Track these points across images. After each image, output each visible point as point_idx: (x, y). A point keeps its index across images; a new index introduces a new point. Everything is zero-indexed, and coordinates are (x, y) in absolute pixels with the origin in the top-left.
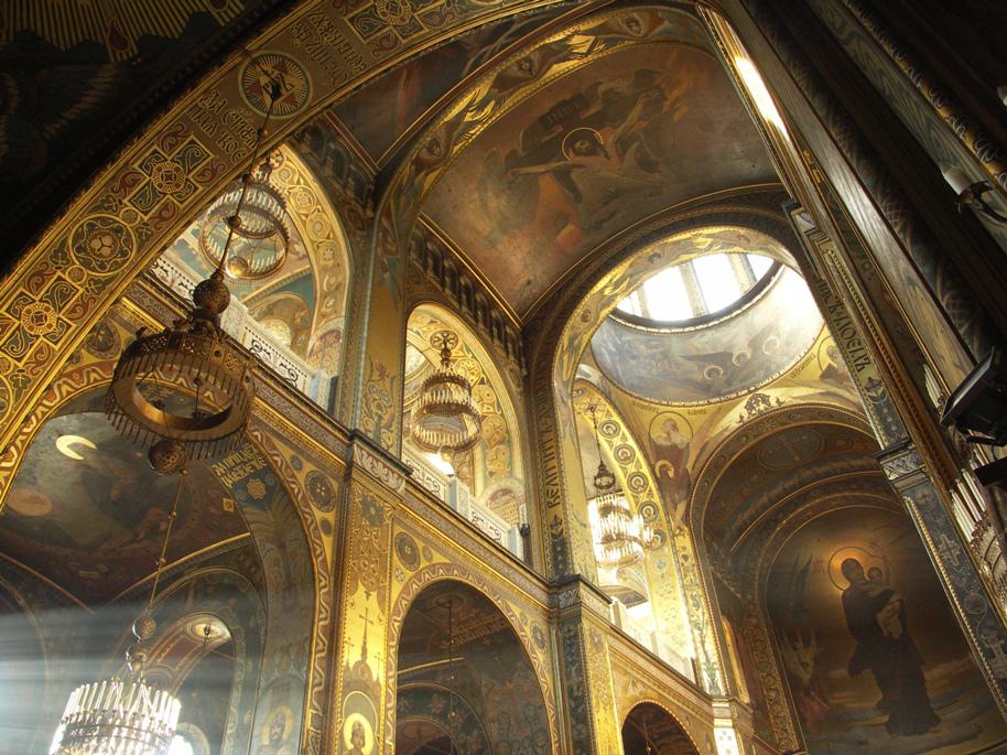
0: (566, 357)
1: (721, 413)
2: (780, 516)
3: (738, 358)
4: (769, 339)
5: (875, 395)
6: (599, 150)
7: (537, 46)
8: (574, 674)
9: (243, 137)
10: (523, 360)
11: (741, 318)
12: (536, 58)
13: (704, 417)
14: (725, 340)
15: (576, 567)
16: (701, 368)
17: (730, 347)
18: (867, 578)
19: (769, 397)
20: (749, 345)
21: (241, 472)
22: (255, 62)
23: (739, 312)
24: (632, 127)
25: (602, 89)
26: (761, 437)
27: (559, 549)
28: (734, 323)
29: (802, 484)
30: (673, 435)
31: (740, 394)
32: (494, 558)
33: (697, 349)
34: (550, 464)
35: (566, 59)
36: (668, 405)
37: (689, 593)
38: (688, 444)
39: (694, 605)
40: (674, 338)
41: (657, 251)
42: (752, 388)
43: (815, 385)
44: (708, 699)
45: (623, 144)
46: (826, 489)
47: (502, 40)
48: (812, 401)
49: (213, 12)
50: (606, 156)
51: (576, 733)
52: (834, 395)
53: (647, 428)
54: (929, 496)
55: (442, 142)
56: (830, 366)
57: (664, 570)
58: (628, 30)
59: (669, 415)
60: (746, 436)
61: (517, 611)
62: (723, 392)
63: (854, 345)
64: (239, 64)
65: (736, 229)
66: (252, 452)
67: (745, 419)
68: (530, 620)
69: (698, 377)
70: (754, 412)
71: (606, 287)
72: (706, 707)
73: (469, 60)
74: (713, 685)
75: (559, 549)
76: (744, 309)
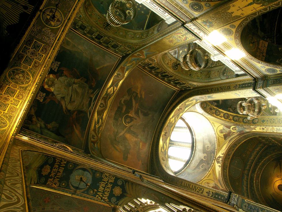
1: (214, 171)
3: (204, 158)
6: (132, 118)
7: (101, 99)
9: (50, 36)
11: (196, 152)
12: (103, 102)
13: (212, 175)
14: (198, 159)
16: (199, 168)
20: (204, 153)
21: (108, 190)
22: (44, 13)
23: (194, 151)
24: (135, 107)
25: (122, 102)
26: (228, 167)
29: (248, 175)
30: (209, 185)
33: (193, 167)
34: (191, 187)
36: (201, 180)
40: (187, 170)
41: (165, 132)
43: (226, 142)
45: (137, 113)
46: (253, 172)
47: (92, 104)
48: (230, 145)
49: (26, 11)
50: (135, 119)
52: (231, 139)
55: (95, 135)
56: (224, 135)
58: (118, 78)
59: (204, 182)
60: (225, 169)
62: (209, 166)
64: (39, 16)
65: (176, 108)
66: (107, 177)
67: (220, 165)
69: (201, 170)
70: (220, 162)
71: (161, 149)
73: (87, 113)
75: (217, 196)
76: (194, 149)
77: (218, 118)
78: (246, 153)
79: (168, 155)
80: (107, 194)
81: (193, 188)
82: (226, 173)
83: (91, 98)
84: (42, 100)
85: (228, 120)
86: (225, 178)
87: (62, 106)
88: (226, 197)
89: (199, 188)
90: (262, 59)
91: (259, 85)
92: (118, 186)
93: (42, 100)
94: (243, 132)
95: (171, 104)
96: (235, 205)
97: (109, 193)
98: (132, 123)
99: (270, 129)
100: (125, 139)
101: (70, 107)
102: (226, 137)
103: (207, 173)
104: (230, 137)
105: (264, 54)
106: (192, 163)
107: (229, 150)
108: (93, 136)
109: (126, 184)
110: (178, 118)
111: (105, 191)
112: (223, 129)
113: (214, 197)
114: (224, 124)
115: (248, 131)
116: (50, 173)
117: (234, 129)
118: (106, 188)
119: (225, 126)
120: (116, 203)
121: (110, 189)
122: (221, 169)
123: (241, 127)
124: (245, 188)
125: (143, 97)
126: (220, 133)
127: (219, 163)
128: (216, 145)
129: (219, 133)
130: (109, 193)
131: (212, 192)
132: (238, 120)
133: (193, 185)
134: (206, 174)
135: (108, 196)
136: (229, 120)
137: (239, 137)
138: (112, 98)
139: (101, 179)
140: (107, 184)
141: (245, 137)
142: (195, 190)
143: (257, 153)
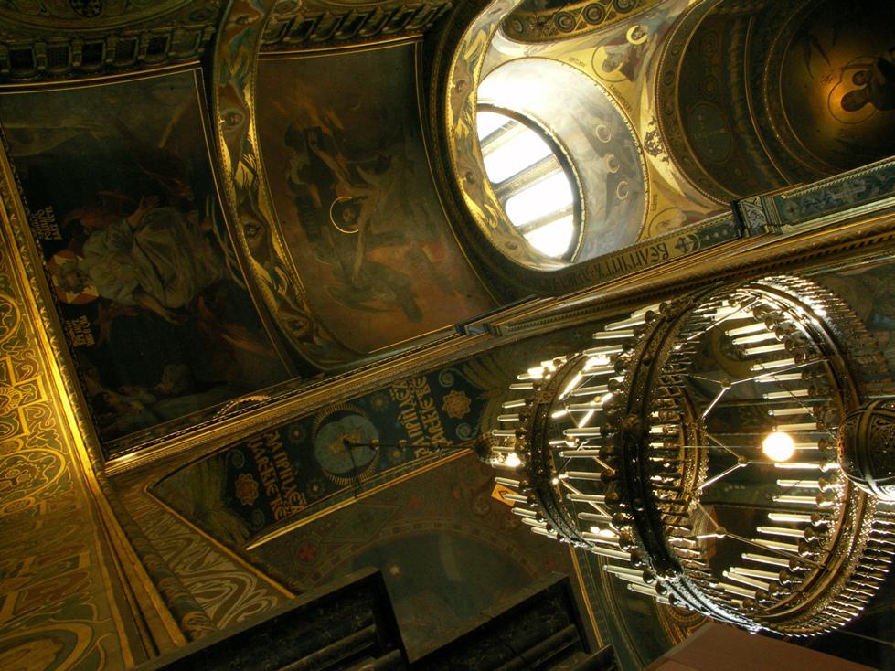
1: (658, 181)
2: (784, 155)
3: (612, 166)
4: (598, 135)
7: (236, 215)
8: (839, 196)
11: (580, 167)
12: (247, 220)
13: (661, 197)
14: (596, 181)
16: (618, 203)
17: (603, 175)
19: (647, 133)
21: (431, 419)
25: (296, 181)
28: (584, 174)
29: (751, 132)
31: (643, 162)
33: (600, 209)
34: (629, 262)
35: (256, 195)
36: (643, 229)
38: (685, 212)
40: (589, 230)
41: (464, 173)
43: (640, 85)
45: (355, 180)
46: (759, 111)
47: (224, 246)
48: (654, 86)
55: (295, 317)
56: (622, 70)
58: (237, 126)
60: (683, 158)
62: (639, 178)
65: (449, 90)
66: (403, 390)
69: (624, 204)
70: (660, 148)
71: (488, 225)
73: (232, 280)
75: (708, 238)
76: (571, 164)
77: (576, 36)
78: (712, 75)
79: (514, 227)
80: (437, 430)
81: (636, 261)
82: (693, 163)
83: (210, 234)
84: (91, 340)
85: (607, 23)
86: (700, 181)
87: (153, 314)
88: (732, 224)
92: (447, 391)
93: (91, 340)
94: (668, 26)
95: (426, 91)
97: (439, 424)
98: (364, 214)
100: (376, 269)
101: (175, 300)
102: (629, 71)
103: (646, 199)
104: (642, 63)
106: (591, 203)
107: (661, 101)
108: (293, 324)
109: (463, 372)
110: (470, 113)
111: (426, 427)
112: (611, 55)
115: (677, 13)
116: (262, 489)
117: (637, 34)
118: (424, 418)
120: (474, 434)
121: (435, 413)
122: (674, 163)
123: (654, 14)
124: (763, 168)
125: (339, 125)
127: (658, 154)
128: (620, 112)
130: (439, 424)
131: (691, 237)
132: (632, 3)
133: (631, 255)
134: (646, 204)
135: (442, 433)
136: (608, 19)
137: (665, 46)
138: (262, 189)
139: (395, 409)
140: (418, 408)
141: (681, 35)
142: (643, 262)
143: (740, 56)
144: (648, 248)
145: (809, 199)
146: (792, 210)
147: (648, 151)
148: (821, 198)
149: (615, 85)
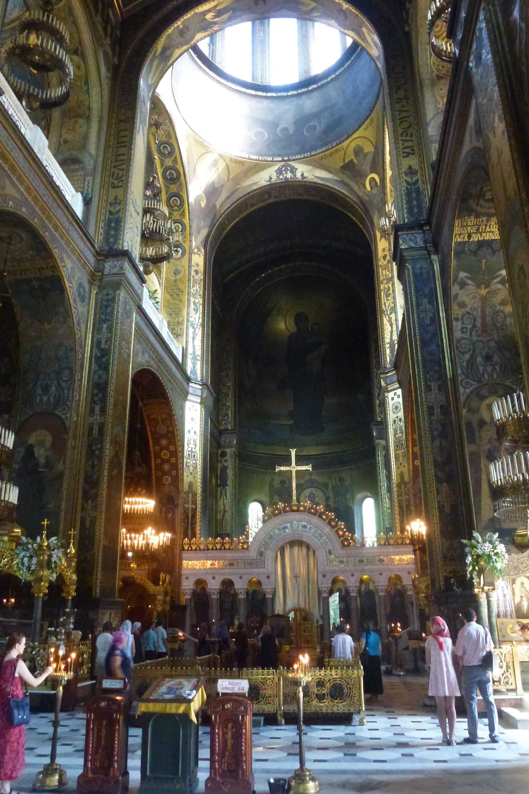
0: (155, 63)
5: (409, 180)
8: (104, 330)
10: (117, 48)
11: (294, 99)
15: (125, 244)
18: (310, 329)
19: (297, 169)
27: (113, 225)
31: (275, 159)
32: (60, 210)
37: (192, 299)
39: (194, 309)
42: (286, 158)
44: (188, 380)
51: (96, 377)
53: (195, 160)
54: (425, 268)
56: (351, 162)
57: (178, 277)
61: (69, 265)
63: (406, 135)
67: (273, 180)
68: (78, 275)
70: (281, 177)
71: (209, 11)
72: (185, 384)
74: (194, 371)
76: (300, 91)
88: (115, 247)
89: (122, 172)
90: (460, 235)
91: (413, 238)
96: (100, 274)
99: (387, 273)
105: (475, 238)
112: (366, 155)
113: (109, 218)
114: (378, 153)
117: (374, 183)
119: (374, 156)
122: (264, 186)
126: (354, 150)
127: (277, 174)
129: (353, 145)
131: (118, 211)
133: (124, 154)
137: (356, 204)
142: (117, 164)
144: (125, 172)
145: (110, 309)
146: (108, 294)
147: (282, 166)
148: (108, 317)
149: (343, 152)
